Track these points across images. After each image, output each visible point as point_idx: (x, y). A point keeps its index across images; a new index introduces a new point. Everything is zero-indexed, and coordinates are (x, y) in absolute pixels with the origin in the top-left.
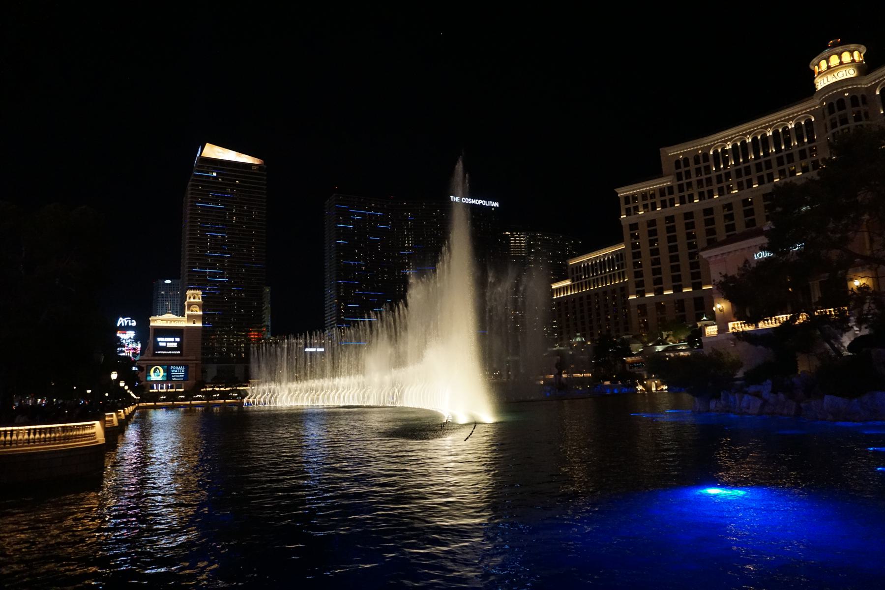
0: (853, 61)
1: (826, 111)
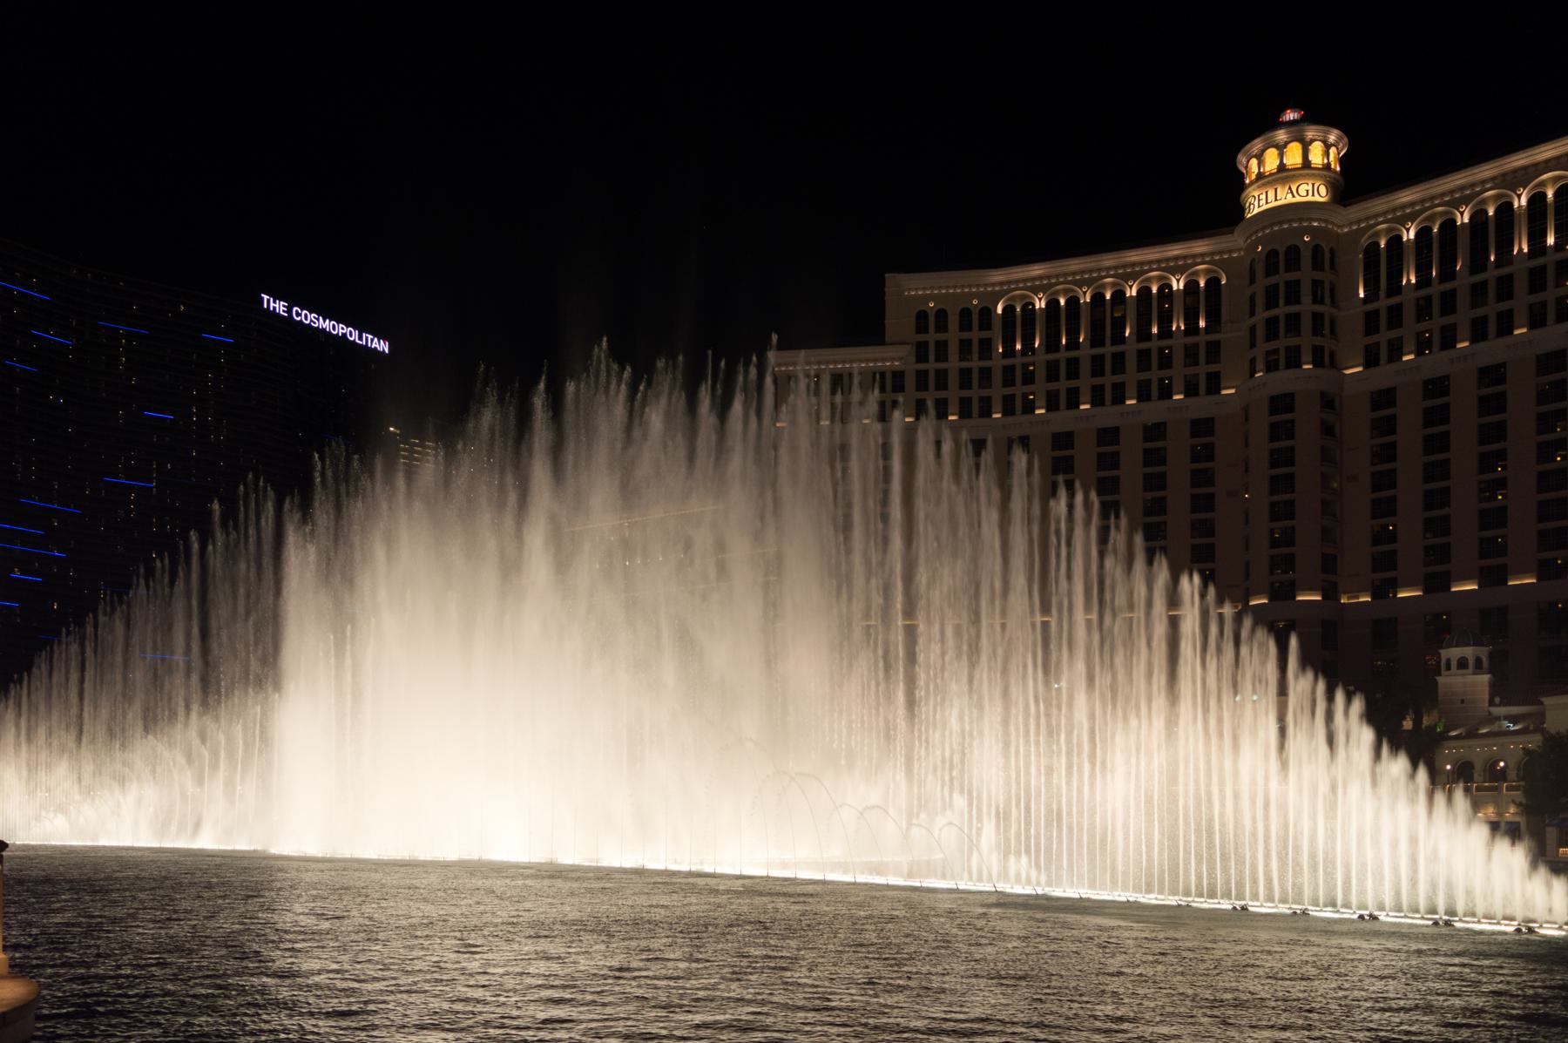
0: (1327, 167)
1: (1260, 269)
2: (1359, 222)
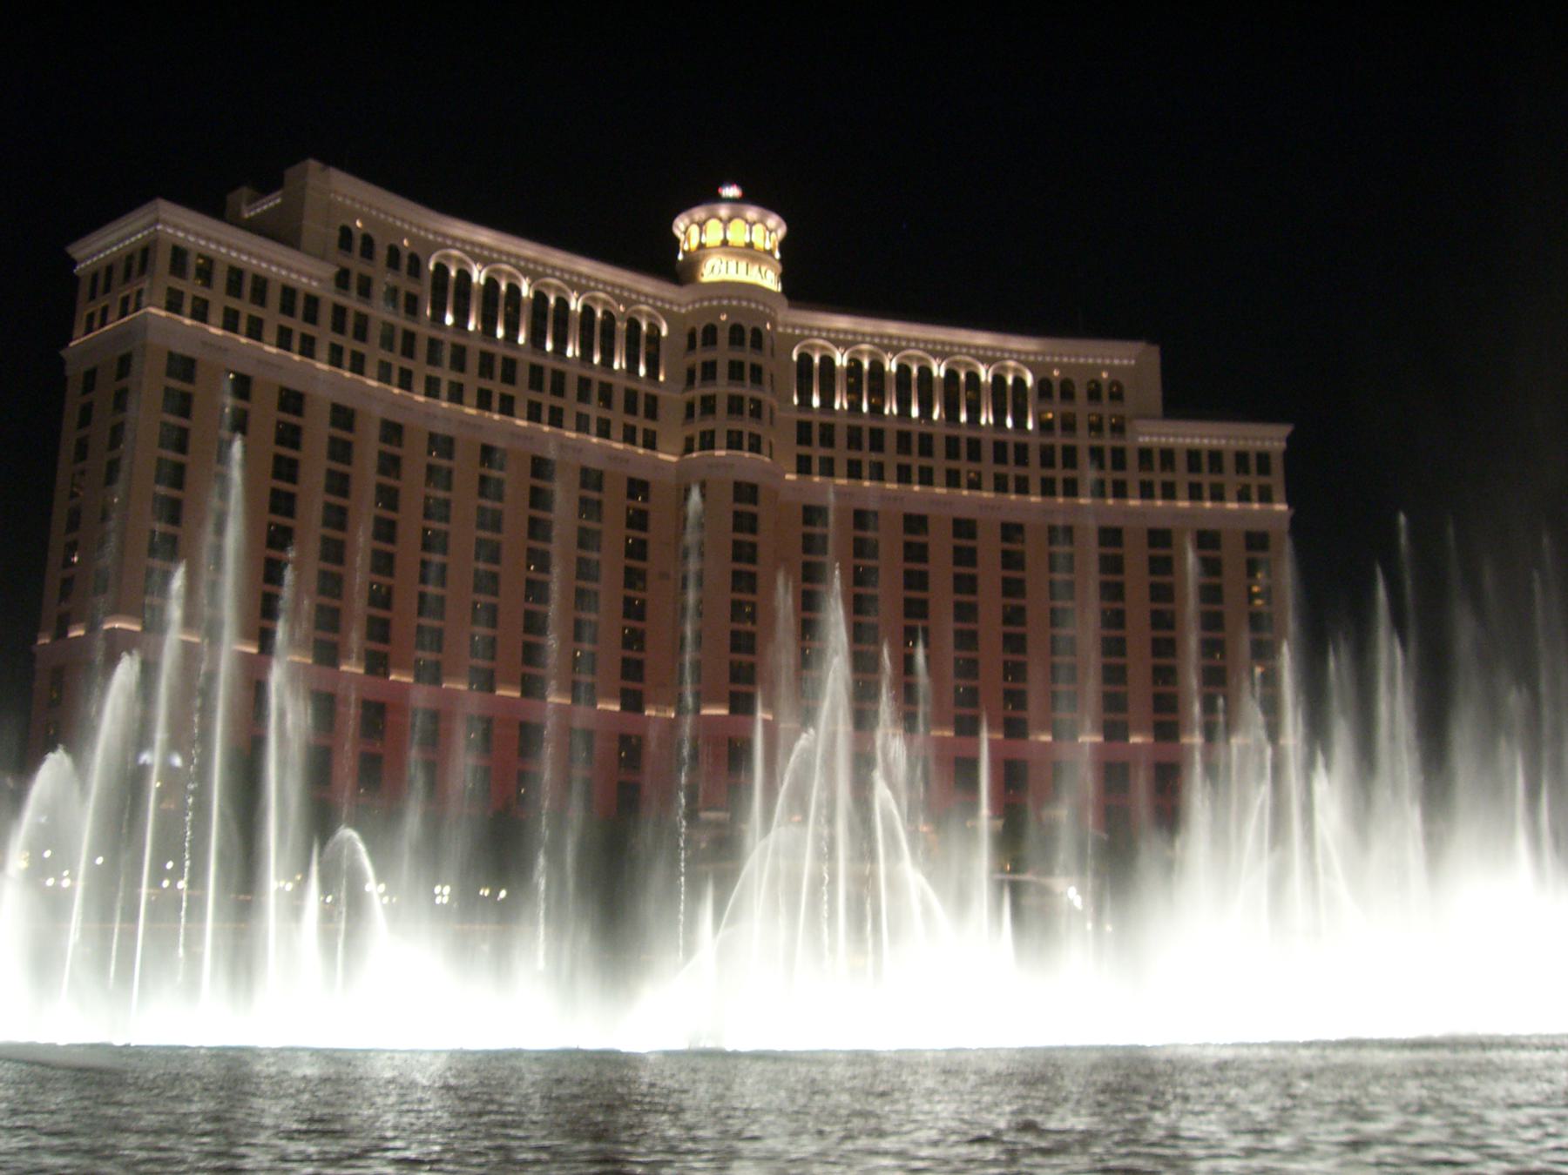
1: (723, 337)
2: (794, 327)
